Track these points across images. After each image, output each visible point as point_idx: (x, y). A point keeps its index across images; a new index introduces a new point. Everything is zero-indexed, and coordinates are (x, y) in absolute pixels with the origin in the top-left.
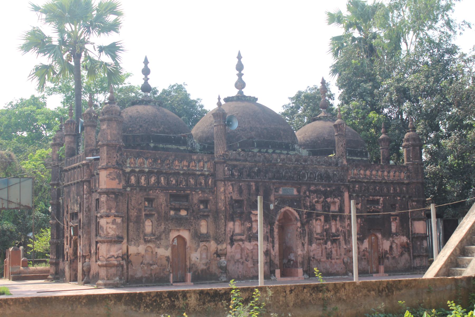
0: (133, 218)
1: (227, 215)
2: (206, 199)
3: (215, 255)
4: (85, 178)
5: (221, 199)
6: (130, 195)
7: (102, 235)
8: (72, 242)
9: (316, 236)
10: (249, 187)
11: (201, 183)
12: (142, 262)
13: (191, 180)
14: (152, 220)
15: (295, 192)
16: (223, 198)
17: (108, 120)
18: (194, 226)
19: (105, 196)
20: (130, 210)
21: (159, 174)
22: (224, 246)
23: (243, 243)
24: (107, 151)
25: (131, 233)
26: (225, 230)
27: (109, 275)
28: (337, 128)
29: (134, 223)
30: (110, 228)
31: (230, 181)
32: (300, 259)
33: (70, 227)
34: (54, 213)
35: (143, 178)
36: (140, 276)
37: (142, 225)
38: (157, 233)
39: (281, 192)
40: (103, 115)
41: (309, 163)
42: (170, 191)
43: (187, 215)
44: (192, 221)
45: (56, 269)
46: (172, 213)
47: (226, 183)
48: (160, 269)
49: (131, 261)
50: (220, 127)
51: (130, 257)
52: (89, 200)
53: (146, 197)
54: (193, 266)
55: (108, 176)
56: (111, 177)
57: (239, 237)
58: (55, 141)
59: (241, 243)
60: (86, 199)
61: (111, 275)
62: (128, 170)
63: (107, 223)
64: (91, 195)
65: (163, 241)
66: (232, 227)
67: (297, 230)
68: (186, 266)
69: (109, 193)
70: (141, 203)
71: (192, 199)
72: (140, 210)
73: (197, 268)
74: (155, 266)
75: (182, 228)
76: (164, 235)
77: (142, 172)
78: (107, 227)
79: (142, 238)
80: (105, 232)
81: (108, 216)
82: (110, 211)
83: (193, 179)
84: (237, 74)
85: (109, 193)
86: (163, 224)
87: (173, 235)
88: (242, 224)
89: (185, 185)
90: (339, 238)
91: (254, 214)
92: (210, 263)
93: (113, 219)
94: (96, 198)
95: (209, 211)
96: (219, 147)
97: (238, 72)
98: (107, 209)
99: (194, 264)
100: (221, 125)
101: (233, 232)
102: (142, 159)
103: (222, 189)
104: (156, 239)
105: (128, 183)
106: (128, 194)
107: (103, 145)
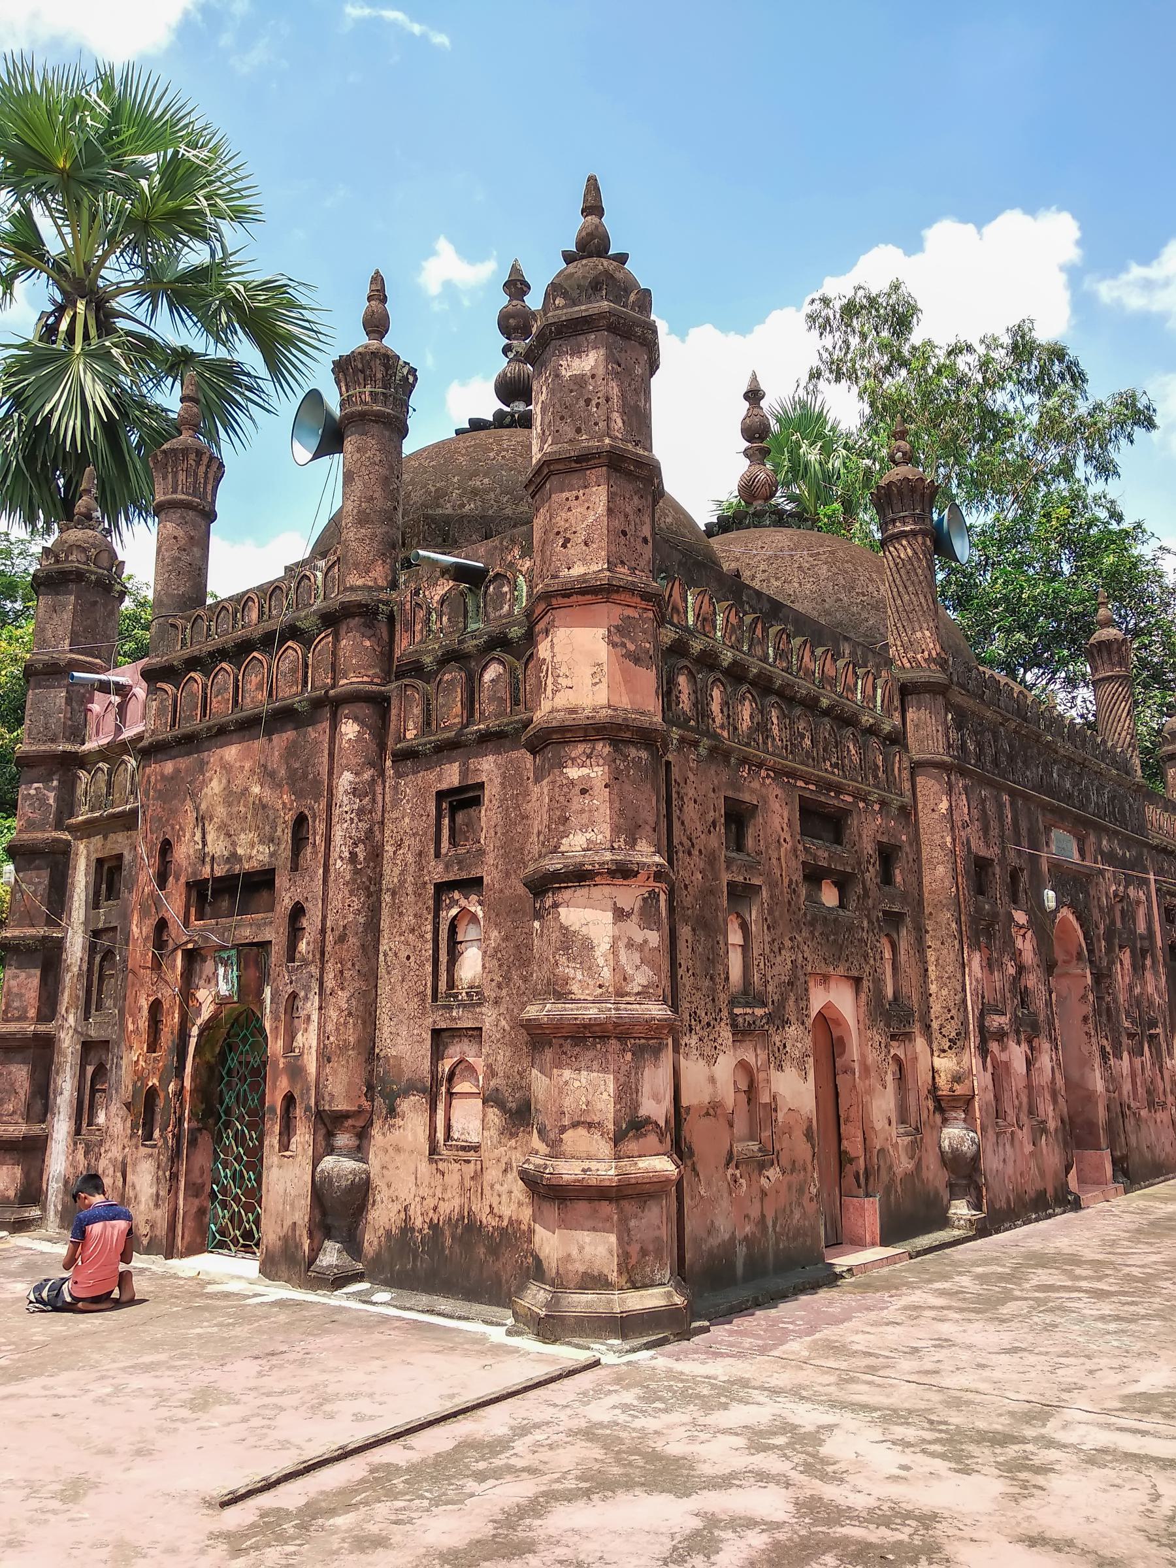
0: (688, 901)
1: (963, 919)
2: (893, 841)
3: (931, 1104)
4: (350, 682)
5: (942, 846)
6: (675, 773)
7: (575, 988)
8: (195, 1031)
9: (1126, 1024)
10: (1000, 806)
11: (877, 767)
12: (731, 1152)
13: (851, 747)
14: (747, 917)
15: (1076, 857)
16: (949, 839)
17: (613, 329)
18: (872, 962)
19: (604, 749)
20: (681, 854)
21: (763, 687)
22: (966, 1058)
23: (1004, 1049)
24: (611, 498)
25: (687, 981)
26: (964, 990)
27: (634, 1249)
28: (1109, 654)
29: (694, 930)
30: (630, 945)
31: (963, 772)
32: (1102, 1115)
33: (193, 957)
34: (34, 893)
35: (716, 693)
36: (727, 1237)
37: (720, 938)
38: (770, 989)
39: (1054, 849)
40: (574, 303)
41: (1089, 746)
42: (800, 783)
43: (842, 905)
44: (865, 935)
45: (26, 1174)
46: (803, 891)
47: (953, 778)
48: (790, 1188)
49: (691, 1153)
50: (924, 543)
51: (685, 1133)
52: (374, 801)
53: (730, 794)
54: (882, 1163)
55: (616, 639)
56: (632, 647)
57: (997, 1021)
58: (57, 561)
59: (994, 1046)
60: (354, 792)
61: (644, 1252)
62: (668, 635)
63: (620, 914)
64: (382, 773)
65: (792, 1031)
66: (980, 975)
67: (1084, 997)
68: (843, 1159)
69: (628, 735)
70: (714, 824)
71: (860, 836)
72: (712, 859)
73: (890, 1168)
74: (773, 1173)
75: (841, 971)
76: (791, 1002)
77: (708, 661)
78: (615, 940)
79: (725, 1014)
80: (606, 973)
81: (623, 872)
82: (632, 842)
83: (856, 741)
84: (746, 452)
85: (628, 735)
86: (788, 944)
87: (818, 999)
88: (990, 965)
89: (836, 766)
90: (1158, 1031)
91: (1018, 925)
92: (922, 1139)
93: (644, 890)
94: (444, 786)
95: (904, 897)
96: (925, 625)
97: (747, 444)
98: (616, 830)
99: (881, 1150)
100: (924, 533)
101: (983, 997)
102: (707, 598)
103: (944, 806)
104: (770, 1018)
105: (670, 708)
106: (668, 763)
107: (580, 459)
